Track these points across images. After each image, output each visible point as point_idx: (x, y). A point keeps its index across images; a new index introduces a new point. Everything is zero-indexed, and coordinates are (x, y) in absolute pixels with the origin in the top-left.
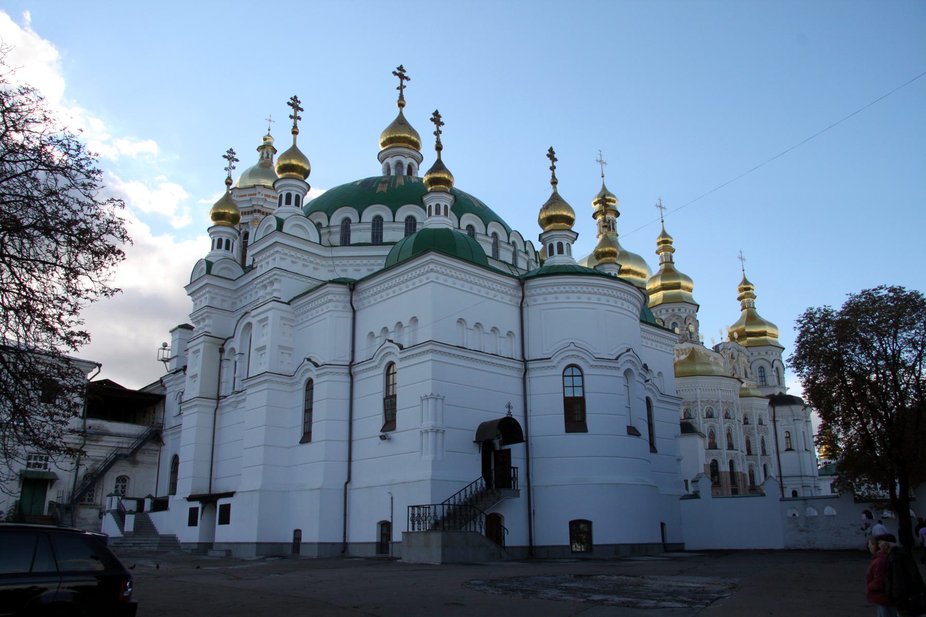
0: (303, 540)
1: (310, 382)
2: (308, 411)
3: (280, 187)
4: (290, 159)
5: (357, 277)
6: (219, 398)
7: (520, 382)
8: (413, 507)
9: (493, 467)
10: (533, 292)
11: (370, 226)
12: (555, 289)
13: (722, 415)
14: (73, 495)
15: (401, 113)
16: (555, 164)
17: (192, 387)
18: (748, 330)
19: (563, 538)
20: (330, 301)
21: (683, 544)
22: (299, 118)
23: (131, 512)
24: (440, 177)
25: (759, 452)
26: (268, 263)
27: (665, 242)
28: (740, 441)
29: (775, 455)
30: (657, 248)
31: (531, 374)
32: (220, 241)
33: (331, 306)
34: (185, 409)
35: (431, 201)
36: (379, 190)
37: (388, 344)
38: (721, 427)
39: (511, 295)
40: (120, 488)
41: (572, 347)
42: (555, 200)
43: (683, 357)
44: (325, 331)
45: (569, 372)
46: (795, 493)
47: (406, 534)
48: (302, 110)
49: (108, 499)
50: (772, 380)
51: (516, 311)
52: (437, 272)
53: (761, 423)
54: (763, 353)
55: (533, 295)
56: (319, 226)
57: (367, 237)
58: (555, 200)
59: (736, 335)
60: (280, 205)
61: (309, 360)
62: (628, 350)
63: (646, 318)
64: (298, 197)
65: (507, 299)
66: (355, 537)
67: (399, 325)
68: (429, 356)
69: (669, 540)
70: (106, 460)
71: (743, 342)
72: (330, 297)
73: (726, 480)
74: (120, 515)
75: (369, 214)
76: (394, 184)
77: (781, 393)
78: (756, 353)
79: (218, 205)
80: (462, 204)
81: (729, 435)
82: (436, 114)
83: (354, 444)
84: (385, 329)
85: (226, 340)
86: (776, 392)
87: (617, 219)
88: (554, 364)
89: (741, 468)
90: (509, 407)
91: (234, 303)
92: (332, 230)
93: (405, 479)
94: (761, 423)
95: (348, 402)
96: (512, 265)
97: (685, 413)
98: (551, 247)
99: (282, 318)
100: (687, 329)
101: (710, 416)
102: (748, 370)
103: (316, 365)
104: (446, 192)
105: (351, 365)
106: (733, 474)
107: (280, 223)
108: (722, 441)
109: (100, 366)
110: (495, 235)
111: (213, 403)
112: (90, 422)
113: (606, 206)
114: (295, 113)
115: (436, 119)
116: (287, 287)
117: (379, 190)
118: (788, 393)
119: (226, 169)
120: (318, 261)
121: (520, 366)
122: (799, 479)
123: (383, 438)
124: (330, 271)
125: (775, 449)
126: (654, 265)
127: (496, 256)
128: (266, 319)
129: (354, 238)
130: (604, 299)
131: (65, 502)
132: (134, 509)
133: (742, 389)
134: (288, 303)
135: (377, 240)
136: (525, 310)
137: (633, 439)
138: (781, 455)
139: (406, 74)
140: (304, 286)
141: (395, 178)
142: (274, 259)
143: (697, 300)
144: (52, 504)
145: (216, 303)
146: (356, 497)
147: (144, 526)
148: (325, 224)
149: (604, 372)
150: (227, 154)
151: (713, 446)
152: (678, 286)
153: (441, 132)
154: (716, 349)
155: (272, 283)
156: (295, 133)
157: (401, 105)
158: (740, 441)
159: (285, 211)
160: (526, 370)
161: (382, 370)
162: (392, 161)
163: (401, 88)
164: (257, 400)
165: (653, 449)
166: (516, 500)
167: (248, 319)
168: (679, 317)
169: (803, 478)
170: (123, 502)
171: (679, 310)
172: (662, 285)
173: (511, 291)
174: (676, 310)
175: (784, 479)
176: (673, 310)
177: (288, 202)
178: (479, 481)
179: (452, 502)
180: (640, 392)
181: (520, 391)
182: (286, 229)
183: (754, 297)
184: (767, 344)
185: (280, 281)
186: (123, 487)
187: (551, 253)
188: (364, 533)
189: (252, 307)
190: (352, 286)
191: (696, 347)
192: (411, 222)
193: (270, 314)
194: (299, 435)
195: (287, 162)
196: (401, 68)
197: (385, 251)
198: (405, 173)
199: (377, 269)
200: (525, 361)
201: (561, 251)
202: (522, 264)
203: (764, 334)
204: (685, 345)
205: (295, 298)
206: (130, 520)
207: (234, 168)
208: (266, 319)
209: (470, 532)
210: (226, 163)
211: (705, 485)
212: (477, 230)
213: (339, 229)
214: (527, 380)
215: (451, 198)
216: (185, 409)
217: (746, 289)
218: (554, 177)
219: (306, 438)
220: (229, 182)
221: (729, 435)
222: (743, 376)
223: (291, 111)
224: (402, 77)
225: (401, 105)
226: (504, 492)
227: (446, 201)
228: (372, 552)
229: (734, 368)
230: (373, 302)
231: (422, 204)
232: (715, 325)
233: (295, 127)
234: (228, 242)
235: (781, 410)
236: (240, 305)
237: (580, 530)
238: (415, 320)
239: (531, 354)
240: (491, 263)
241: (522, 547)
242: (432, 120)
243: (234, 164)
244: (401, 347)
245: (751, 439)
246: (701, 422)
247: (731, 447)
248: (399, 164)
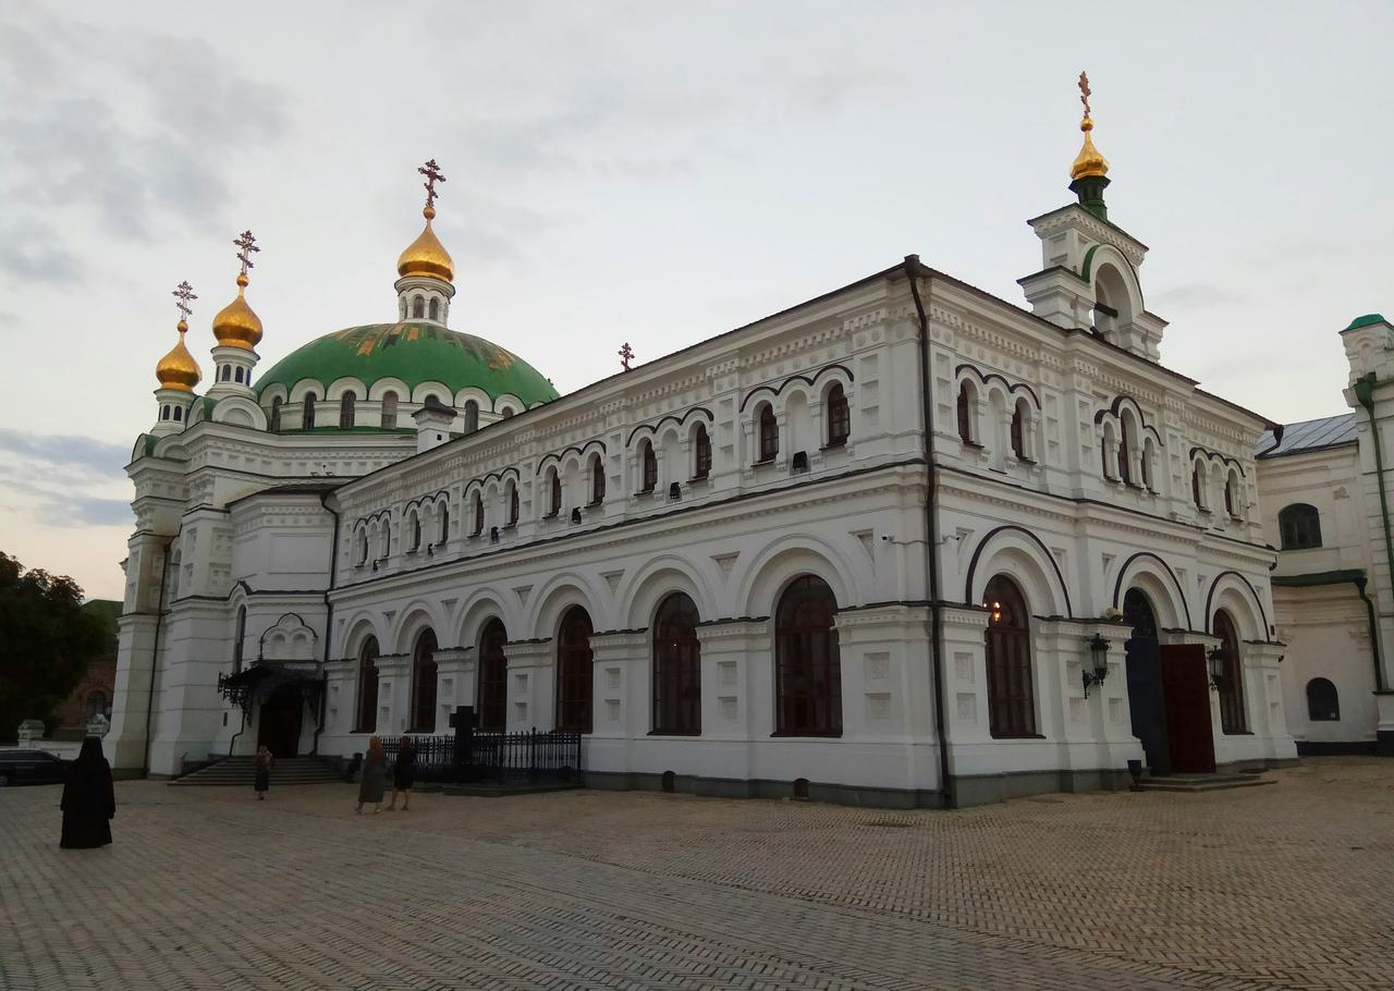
1: (243, 610)
11: (338, 406)
15: (428, 227)
32: (167, 409)
36: (360, 352)
60: (217, 381)
61: (243, 583)
72: (263, 510)
75: (336, 392)
99: (215, 529)
111: (153, 620)
116: (224, 490)
117: (360, 352)
135: (347, 426)
142: (206, 454)
145: (163, 492)
150: (178, 290)
155: (204, 484)
157: (429, 216)
162: (410, 295)
182: (218, 415)
185: (213, 483)
196: (432, 164)
212: (481, 408)
213: (301, 408)
224: (433, 176)
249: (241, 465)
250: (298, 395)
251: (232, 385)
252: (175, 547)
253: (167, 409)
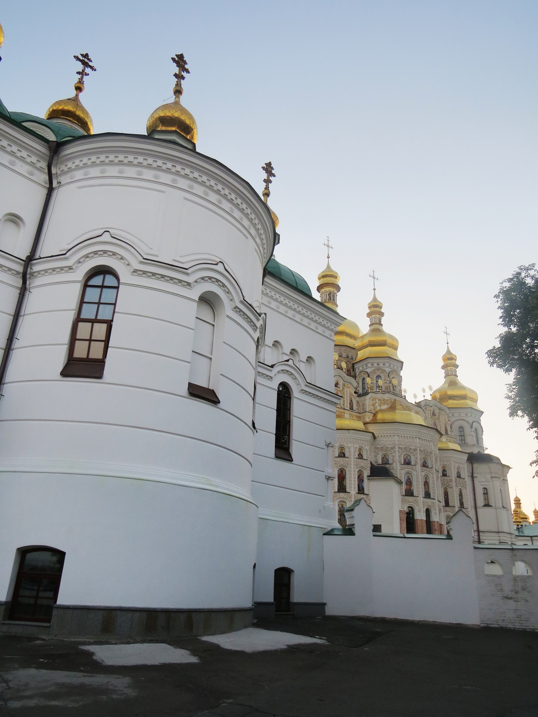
18: (450, 392)
25: (457, 504)
28: (437, 492)
29: (473, 510)
30: (368, 311)
50: (470, 439)
53: (459, 476)
54: (463, 414)
77: (479, 452)
78: (456, 415)
81: (426, 484)
86: (475, 451)
94: (459, 476)
97: (383, 458)
100: (390, 382)
102: (449, 428)
108: (418, 489)
122: (496, 535)
125: (473, 505)
138: (478, 510)
143: (401, 358)
151: (409, 493)
152: (383, 344)
158: (437, 492)
168: (383, 371)
169: (501, 534)
171: (384, 364)
175: (481, 534)
176: (378, 364)
183: (457, 366)
204: (387, 396)
245: (449, 490)
246: (399, 468)
247: (427, 495)
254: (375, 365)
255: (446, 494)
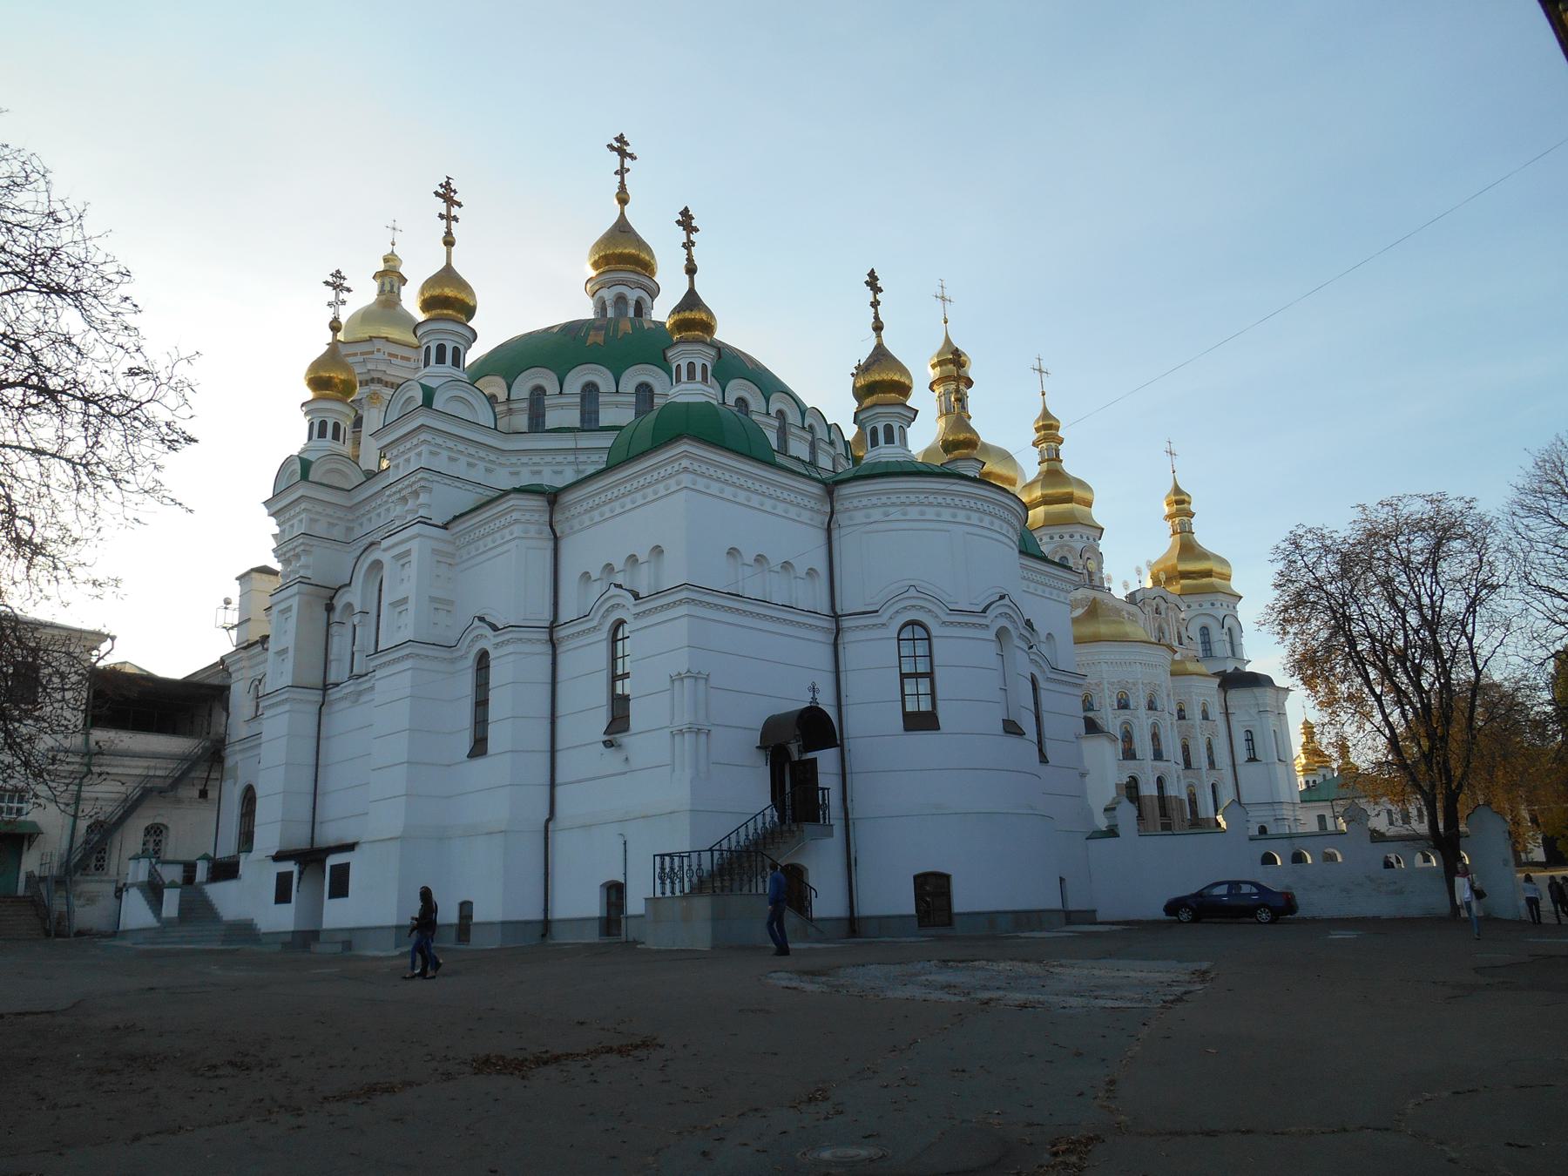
0: (475, 919)
2: (481, 704)
3: (426, 334)
4: (442, 286)
5: (559, 483)
6: (325, 687)
7: (829, 650)
8: (662, 856)
9: (788, 789)
10: (847, 504)
12: (884, 499)
13: (1143, 703)
14: (68, 861)
16: (879, 297)
17: (279, 673)
18: (1183, 567)
19: (905, 904)
20: (517, 521)
21: (1094, 911)
22: (456, 219)
23: (173, 885)
24: (694, 318)
26: (408, 460)
27: (1048, 429)
28: (1172, 748)
30: (1035, 436)
31: (847, 637)
32: (323, 424)
33: (517, 530)
34: (266, 708)
35: (680, 357)
36: (590, 340)
37: (613, 591)
38: (1142, 724)
39: (812, 509)
40: (151, 846)
41: (912, 592)
42: (880, 355)
43: (1079, 612)
44: (505, 573)
45: (906, 634)
46: (1263, 830)
47: (652, 901)
48: (460, 205)
49: (132, 864)
50: (1220, 647)
51: (821, 537)
52: (694, 472)
53: (1205, 717)
55: (848, 510)
56: (492, 399)
57: (573, 418)
58: (880, 355)
59: (1163, 577)
60: (427, 364)
61: (481, 619)
62: (1002, 597)
63: (1028, 549)
64: (456, 351)
65: (806, 516)
66: (563, 909)
67: (633, 559)
68: (683, 610)
69: (1072, 906)
70: (126, 800)
71: (1175, 588)
72: (515, 515)
73: (1153, 811)
74: (154, 891)
75: (576, 381)
76: (616, 330)
79: (317, 365)
80: (731, 365)
81: (1155, 737)
82: (685, 213)
83: (560, 757)
84: (609, 568)
85: (337, 591)
87: (969, 392)
88: (884, 619)
89: (1176, 790)
90: (814, 689)
91: (349, 530)
92: (514, 406)
93: (644, 810)
95: (548, 688)
96: (811, 463)
98: (874, 432)
101: (1123, 705)
102: (1183, 631)
103: (494, 628)
104: (704, 342)
105: (553, 627)
106: (1162, 797)
107: (429, 396)
108: (1143, 746)
109: (113, 638)
110: (781, 413)
111: (316, 696)
112: (99, 735)
113: (954, 369)
114: (449, 211)
115: (686, 221)
117: (590, 340)
118: (1248, 668)
119: (330, 304)
120: (492, 457)
121: (828, 624)
123: (609, 744)
124: (512, 474)
126: (1030, 466)
127: (783, 448)
128: (408, 553)
129: (552, 419)
130: (961, 516)
131: (55, 871)
132: (179, 880)
133: (1174, 662)
134: (445, 527)
135: (589, 423)
136: (835, 534)
137: (1013, 741)
139: (629, 150)
140: (467, 499)
141: (616, 320)
143: (1099, 522)
144: (30, 877)
145: (320, 529)
146: (563, 843)
147: (197, 909)
148: (502, 397)
149: (970, 633)
150: (330, 280)
151: (1129, 754)
152: (1068, 499)
153: (693, 244)
154: (1132, 598)
155: (416, 494)
156: (449, 242)
158: (1172, 748)
159: (436, 375)
160: (838, 631)
161: (604, 633)
162: (608, 295)
163: (622, 172)
164: (394, 685)
165: (1043, 759)
166: (829, 840)
167: (375, 555)
170: (158, 867)
172: (1043, 496)
173: (812, 504)
174: (1067, 537)
176: (1061, 537)
177: (441, 359)
178: (768, 812)
179: (725, 847)
180: (1023, 664)
181: (828, 664)
183: (1192, 515)
184: (1213, 590)
186: (157, 843)
187: (875, 443)
188: (579, 901)
189: (382, 533)
190: (553, 497)
191: (1099, 595)
192: (644, 390)
193: (414, 545)
194: (466, 742)
195: (437, 292)
197: (606, 441)
198: (631, 313)
199: (591, 470)
200: (836, 617)
201: (889, 439)
202: (825, 462)
203: (1208, 574)
204: (1081, 593)
205: (455, 518)
206: (171, 902)
207: (344, 302)
208: (408, 553)
209: (758, 895)
210: (330, 294)
211: (1127, 812)
212: (753, 407)
213: (525, 405)
214: (840, 648)
215: (713, 353)
216: (266, 708)
217: (1180, 504)
218: (876, 317)
219: (479, 747)
220: (335, 326)
221: (1155, 737)
222: (1176, 643)
223: (442, 207)
225: (623, 199)
226: (809, 828)
227: (703, 358)
228: (592, 936)
229: (1161, 630)
230: (587, 523)
231: (664, 364)
232: (1129, 559)
233: (449, 233)
234: (336, 426)
235: (1237, 697)
236: (358, 532)
237: (933, 890)
238: (658, 550)
239: (844, 606)
240: (779, 459)
241: (838, 919)
242: (678, 222)
243: (344, 295)
244: (636, 596)
246: (1110, 716)
247: (1158, 755)
248: (621, 300)
249: (460, 469)
250: (523, 387)
251: (447, 368)
252: (339, 603)
253: (323, 424)
254: (1057, 538)
255: (1186, 749)
